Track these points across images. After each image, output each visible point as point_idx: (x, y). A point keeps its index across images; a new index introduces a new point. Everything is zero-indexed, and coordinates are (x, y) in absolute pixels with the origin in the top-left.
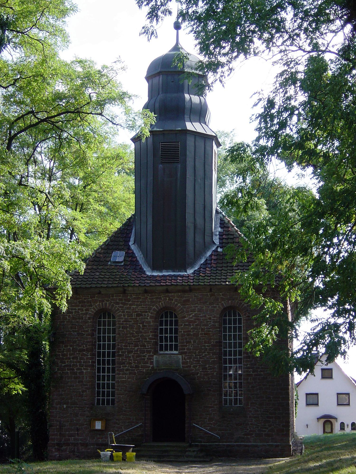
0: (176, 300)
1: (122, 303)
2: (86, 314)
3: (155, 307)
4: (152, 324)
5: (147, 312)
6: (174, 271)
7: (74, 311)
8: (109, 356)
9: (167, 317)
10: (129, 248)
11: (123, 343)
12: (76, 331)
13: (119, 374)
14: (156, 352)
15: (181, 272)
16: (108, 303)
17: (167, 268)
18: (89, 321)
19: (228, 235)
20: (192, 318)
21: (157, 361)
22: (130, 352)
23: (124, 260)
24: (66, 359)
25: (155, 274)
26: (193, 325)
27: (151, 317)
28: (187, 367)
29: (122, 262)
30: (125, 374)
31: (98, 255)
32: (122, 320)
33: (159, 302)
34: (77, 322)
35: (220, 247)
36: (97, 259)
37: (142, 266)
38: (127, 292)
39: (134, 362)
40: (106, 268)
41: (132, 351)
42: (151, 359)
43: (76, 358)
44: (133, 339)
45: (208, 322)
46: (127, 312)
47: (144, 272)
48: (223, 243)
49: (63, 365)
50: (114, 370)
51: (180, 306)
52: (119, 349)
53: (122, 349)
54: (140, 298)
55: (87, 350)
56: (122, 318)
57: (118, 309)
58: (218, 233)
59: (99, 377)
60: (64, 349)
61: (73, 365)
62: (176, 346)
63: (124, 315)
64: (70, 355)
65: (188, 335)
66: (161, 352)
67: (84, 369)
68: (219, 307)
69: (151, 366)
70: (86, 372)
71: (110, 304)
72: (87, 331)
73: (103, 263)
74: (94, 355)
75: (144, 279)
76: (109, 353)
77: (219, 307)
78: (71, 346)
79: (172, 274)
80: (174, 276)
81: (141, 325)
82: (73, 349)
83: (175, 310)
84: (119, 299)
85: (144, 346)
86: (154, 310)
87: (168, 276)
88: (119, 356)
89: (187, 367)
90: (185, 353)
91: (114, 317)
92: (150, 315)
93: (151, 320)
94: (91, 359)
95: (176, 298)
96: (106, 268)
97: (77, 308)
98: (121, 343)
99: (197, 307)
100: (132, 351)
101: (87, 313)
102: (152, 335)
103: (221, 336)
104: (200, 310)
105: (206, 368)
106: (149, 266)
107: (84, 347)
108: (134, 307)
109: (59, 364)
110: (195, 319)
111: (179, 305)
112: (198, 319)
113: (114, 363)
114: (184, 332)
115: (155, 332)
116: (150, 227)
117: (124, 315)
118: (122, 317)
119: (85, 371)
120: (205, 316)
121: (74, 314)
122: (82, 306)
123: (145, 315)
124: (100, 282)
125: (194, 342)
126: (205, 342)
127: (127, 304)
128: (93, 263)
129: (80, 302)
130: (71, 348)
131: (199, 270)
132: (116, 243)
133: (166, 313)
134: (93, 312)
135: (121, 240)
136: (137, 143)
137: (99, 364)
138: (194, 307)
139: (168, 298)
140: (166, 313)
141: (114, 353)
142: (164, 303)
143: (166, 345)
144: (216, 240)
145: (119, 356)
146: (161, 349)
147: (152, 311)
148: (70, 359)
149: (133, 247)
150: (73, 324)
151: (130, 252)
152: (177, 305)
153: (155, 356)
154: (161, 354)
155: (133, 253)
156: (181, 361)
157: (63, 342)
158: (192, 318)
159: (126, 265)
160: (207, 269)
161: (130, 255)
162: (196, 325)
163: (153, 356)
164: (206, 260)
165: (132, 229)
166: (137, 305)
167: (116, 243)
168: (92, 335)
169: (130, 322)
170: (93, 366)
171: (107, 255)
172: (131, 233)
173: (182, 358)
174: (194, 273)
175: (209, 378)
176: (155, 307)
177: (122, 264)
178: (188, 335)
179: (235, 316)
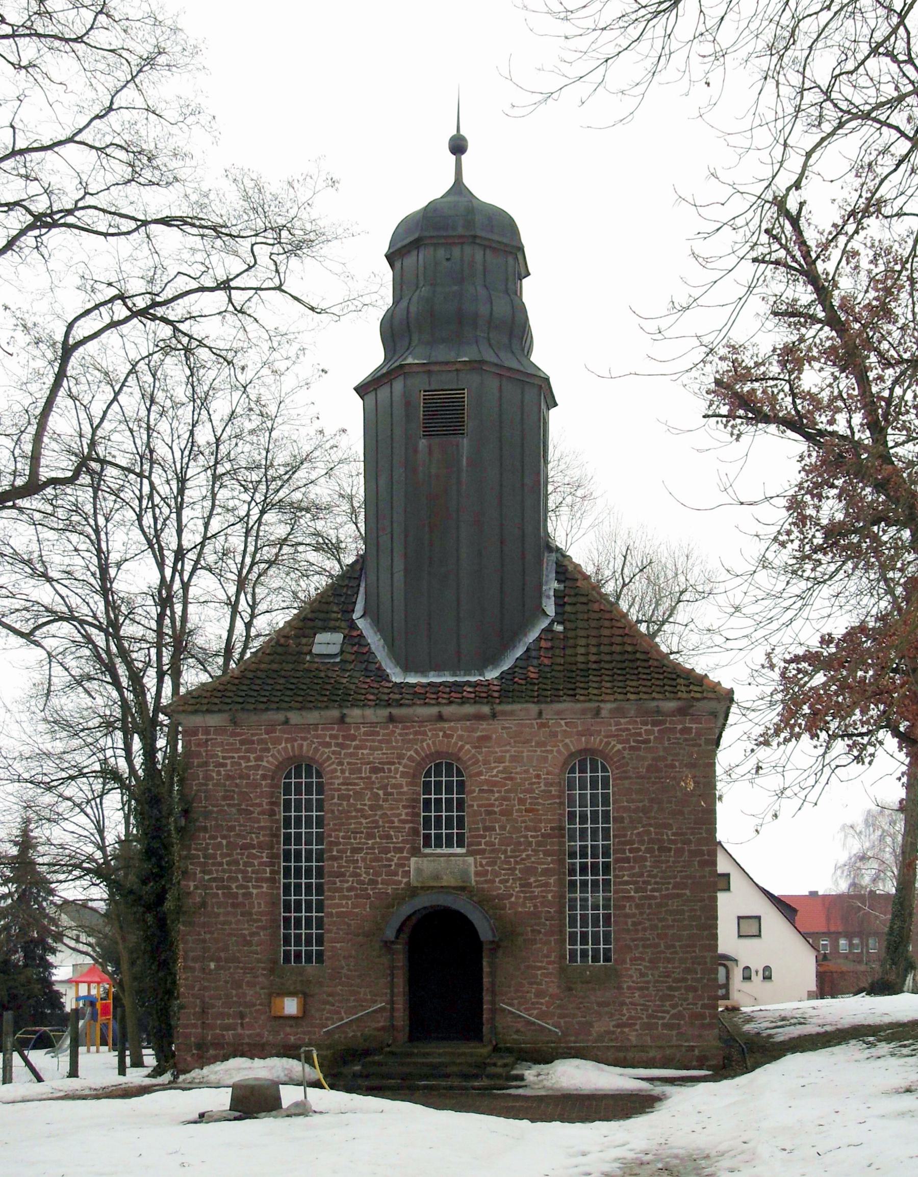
0: (460, 738)
1: (337, 745)
2: (257, 767)
3: (412, 753)
4: (405, 789)
5: (393, 763)
6: (454, 675)
7: (228, 761)
8: (309, 859)
9: (438, 774)
10: (353, 626)
11: (339, 830)
12: (233, 805)
13: (333, 898)
14: (415, 852)
15: (470, 675)
16: (305, 743)
17: (438, 668)
18: (263, 783)
19: (576, 595)
20: (496, 776)
21: (419, 871)
22: (355, 850)
23: (342, 652)
24: (214, 864)
25: (412, 679)
26: (499, 792)
27: (404, 775)
28: (486, 882)
29: (335, 655)
30: (348, 898)
31: (282, 641)
32: (337, 782)
33: (423, 741)
34: (237, 785)
35: (559, 623)
36: (280, 650)
37: (383, 665)
38: (348, 720)
39: (367, 874)
40: (302, 667)
41: (362, 849)
42: (403, 865)
43: (237, 863)
44: (364, 821)
45: (534, 783)
46: (349, 763)
47: (386, 678)
48: (563, 613)
49: (207, 877)
50: (320, 889)
51: (469, 751)
52: (331, 843)
53: (340, 843)
54: (378, 734)
55: (260, 846)
56: (338, 778)
57: (329, 758)
58: (552, 593)
59: (287, 904)
60: (207, 844)
61: (230, 878)
62: (461, 837)
63: (343, 771)
64: (223, 855)
65: (489, 813)
66: (427, 851)
67: (255, 887)
68: (559, 752)
69: (405, 880)
70: (257, 895)
71: (309, 746)
72: (260, 805)
73: (294, 658)
74: (274, 856)
75: (386, 690)
76: (309, 852)
77: (559, 752)
78: (224, 837)
79: (451, 679)
80: (455, 684)
81: (381, 792)
82: (229, 843)
83: (459, 759)
84: (331, 736)
85: (389, 837)
86: (411, 758)
87: (441, 684)
88: (334, 858)
89: (486, 882)
90: (482, 852)
91: (319, 775)
92: (401, 769)
93: (403, 781)
94: (272, 864)
95: (460, 732)
96: (302, 667)
97: (236, 755)
98: (336, 830)
99: (508, 751)
100: (362, 849)
101: (259, 766)
102: (407, 814)
103: (562, 815)
104: (514, 759)
105: (529, 885)
106: (398, 663)
107: (252, 839)
108: (365, 752)
109: (198, 876)
110: (505, 778)
111: (468, 747)
112: (511, 779)
113: (320, 874)
114: (479, 806)
115: (414, 807)
116: (399, 576)
117: (343, 771)
118: (339, 774)
119: (255, 891)
120: (527, 771)
121: (229, 767)
122: (247, 751)
123: (390, 770)
124: (287, 699)
125: (503, 828)
126: (527, 829)
127: (348, 747)
128: (271, 657)
129: (242, 743)
130: (224, 842)
131: (511, 671)
132: (322, 616)
133: (298, 768)
134: (272, 764)
135: (335, 609)
136: (371, 397)
137: (287, 875)
138: (502, 751)
139: (441, 734)
140: (298, 768)
141: (320, 853)
142: (434, 743)
143: (438, 837)
144: (551, 610)
145: (334, 858)
146: (427, 844)
147: (405, 761)
148: (221, 864)
149: (361, 623)
150: (226, 791)
151: (355, 633)
152: (462, 747)
153: (413, 860)
154: (426, 855)
155: (361, 636)
156: (472, 869)
157: (205, 829)
158: (496, 776)
159: (346, 661)
160: (531, 669)
161: (354, 639)
162: (507, 791)
163: (408, 859)
164: (528, 650)
165: (359, 585)
166: (371, 748)
167: (322, 616)
168: (272, 813)
169: (355, 784)
170: (273, 881)
171: (304, 641)
172: (357, 593)
173: (475, 863)
174: (501, 677)
175: (535, 906)
176: (412, 753)
177: (338, 660)
178: (489, 813)
179: (594, 770)
